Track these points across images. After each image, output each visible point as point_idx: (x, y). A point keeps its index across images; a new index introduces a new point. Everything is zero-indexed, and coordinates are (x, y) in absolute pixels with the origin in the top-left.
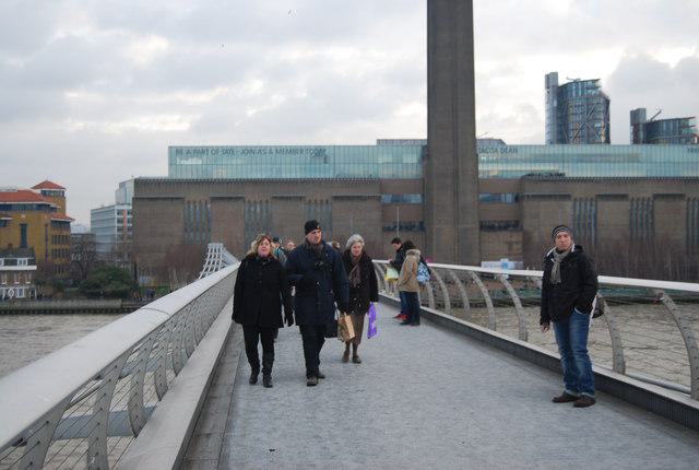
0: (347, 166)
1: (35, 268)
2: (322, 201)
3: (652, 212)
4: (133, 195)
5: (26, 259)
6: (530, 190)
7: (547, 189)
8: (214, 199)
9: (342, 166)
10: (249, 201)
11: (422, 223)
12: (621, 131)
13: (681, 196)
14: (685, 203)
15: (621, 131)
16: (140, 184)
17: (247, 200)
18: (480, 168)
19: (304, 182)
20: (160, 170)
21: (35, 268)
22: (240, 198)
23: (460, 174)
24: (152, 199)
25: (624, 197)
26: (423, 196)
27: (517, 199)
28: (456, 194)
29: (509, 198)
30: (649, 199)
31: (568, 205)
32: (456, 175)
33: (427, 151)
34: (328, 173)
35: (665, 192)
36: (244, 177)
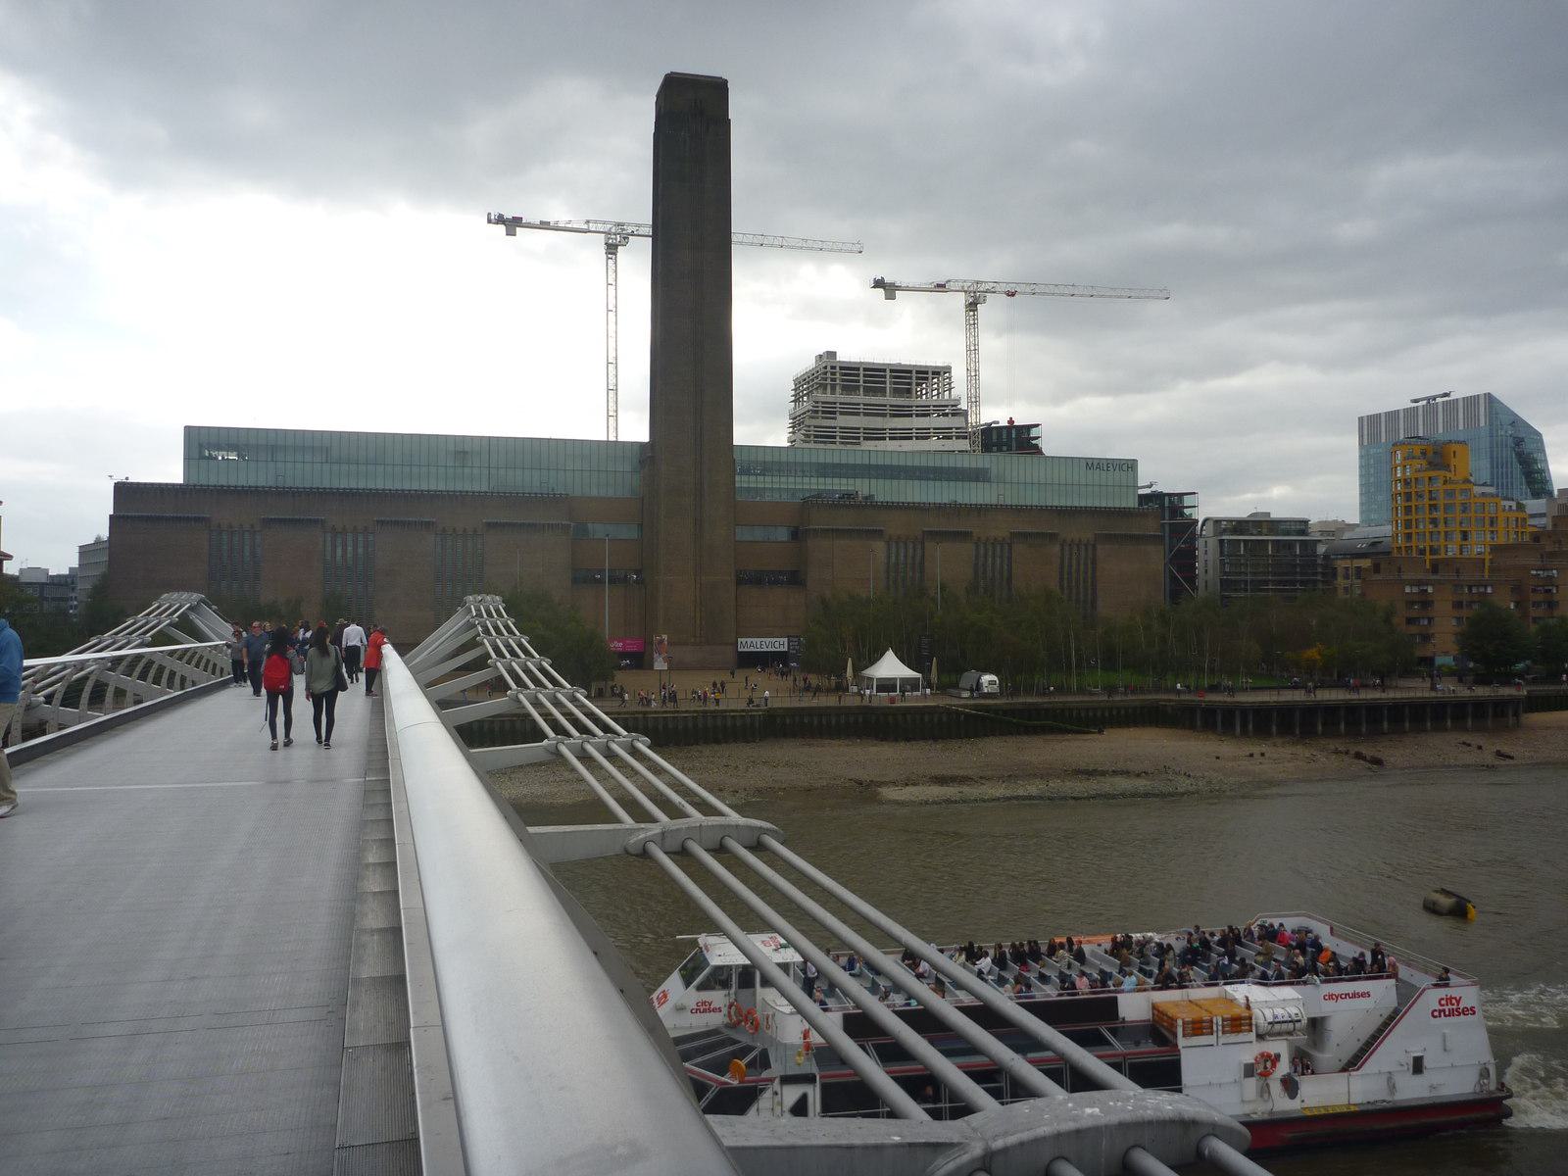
2: (465, 530)
3: (1010, 558)
9: (502, 472)
14: (1057, 548)
16: (126, 493)
18: (741, 481)
19: (434, 497)
20: (171, 471)
22: (316, 521)
24: (148, 519)
25: (964, 536)
26: (641, 526)
27: (796, 535)
29: (782, 534)
31: (879, 546)
35: (1030, 530)
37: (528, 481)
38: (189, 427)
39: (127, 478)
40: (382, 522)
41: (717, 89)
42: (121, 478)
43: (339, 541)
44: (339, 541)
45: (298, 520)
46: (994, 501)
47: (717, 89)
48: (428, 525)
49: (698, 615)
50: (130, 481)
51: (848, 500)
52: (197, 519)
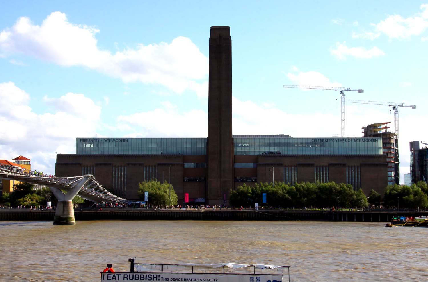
7: (270, 161)
8: (97, 165)
9: (165, 148)
10: (115, 166)
11: (205, 178)
13: (344, 165)
22: (110, 164)
30: (326, 166)
36: (115, 153)
37: (174, 151)
38: (78, 138)
39: (60, 153)
40: (129, 164)
41: (226, 30)
42: (58, 153)
43: (117, 169)
44: (117, 169)
45: (106, 164)
46: (327, 153)
47: (226, 30)
48: (141, 164)
49: (220, 191)
50: (62, 153)
51: (271, 155)
52: (78, 164)
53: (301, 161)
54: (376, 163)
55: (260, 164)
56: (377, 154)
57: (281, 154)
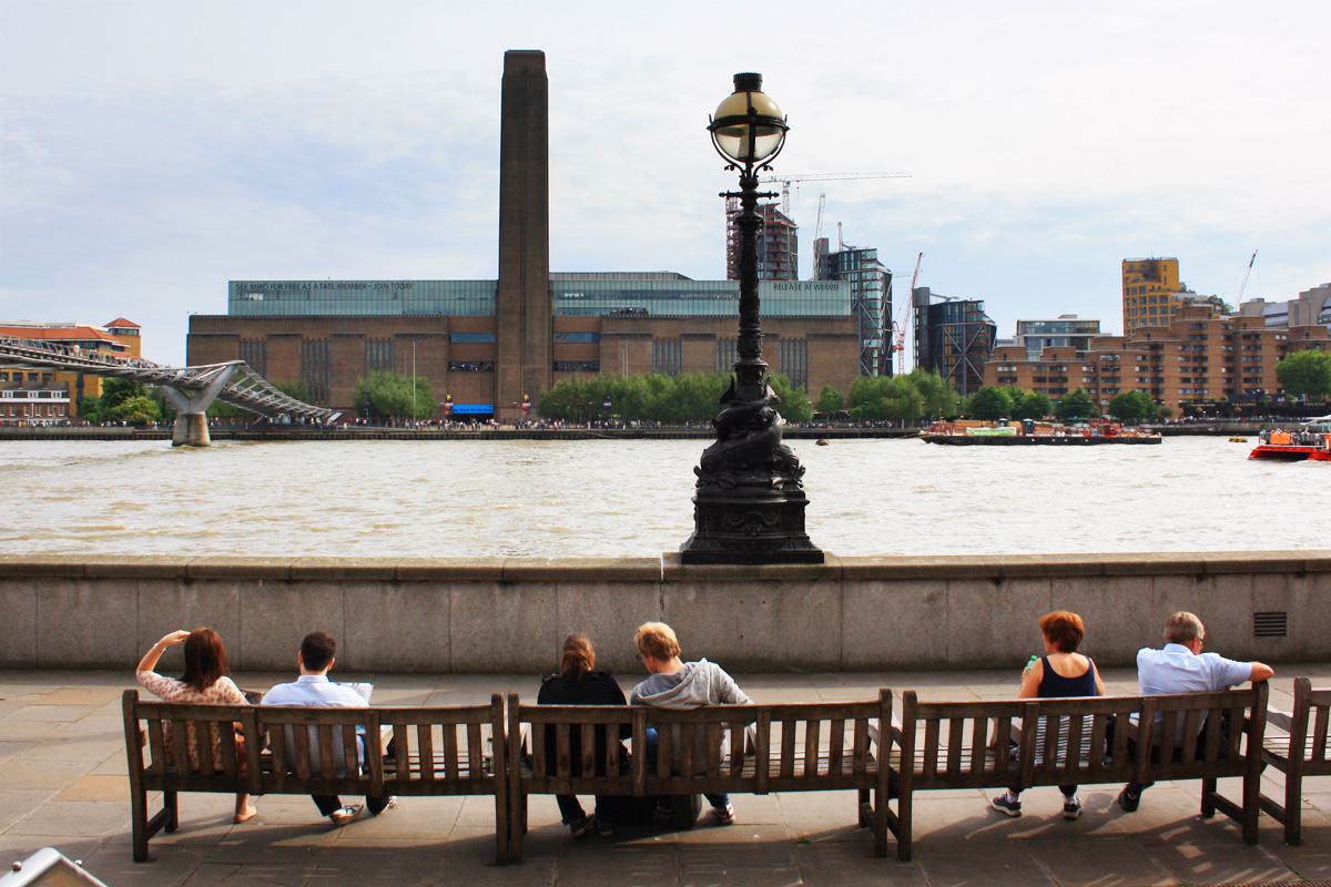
0: (416, 302)
1: (68, 400)
4: (187, 332)
5: (60, 392)
6: (608, 329)
12: (806, 268)
15: (806, 268)
17: (305, 338)
19: (366, 319)
20: (219, 306)
21: (68, 400)
23: (528, 311)
25: (711, 337)
28: (523, 331)
31: (649, 345)
32: (523, 312)
33: (498, 287)
34: (393, 309)
37: (428, 307)
40: (334, 335)
47: (539, 57)
53: (690, 329)
54: (837, 332)
55: (605, 335)
56: (840, 313)
57: (650, 313)
